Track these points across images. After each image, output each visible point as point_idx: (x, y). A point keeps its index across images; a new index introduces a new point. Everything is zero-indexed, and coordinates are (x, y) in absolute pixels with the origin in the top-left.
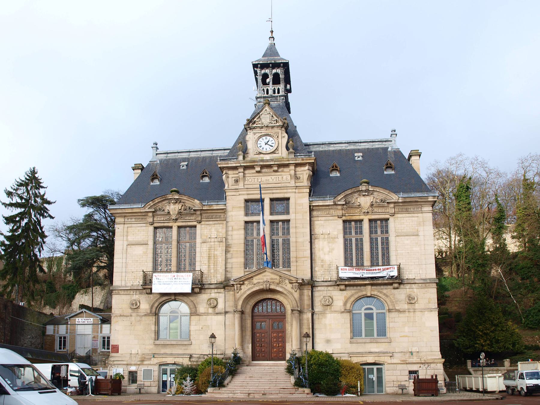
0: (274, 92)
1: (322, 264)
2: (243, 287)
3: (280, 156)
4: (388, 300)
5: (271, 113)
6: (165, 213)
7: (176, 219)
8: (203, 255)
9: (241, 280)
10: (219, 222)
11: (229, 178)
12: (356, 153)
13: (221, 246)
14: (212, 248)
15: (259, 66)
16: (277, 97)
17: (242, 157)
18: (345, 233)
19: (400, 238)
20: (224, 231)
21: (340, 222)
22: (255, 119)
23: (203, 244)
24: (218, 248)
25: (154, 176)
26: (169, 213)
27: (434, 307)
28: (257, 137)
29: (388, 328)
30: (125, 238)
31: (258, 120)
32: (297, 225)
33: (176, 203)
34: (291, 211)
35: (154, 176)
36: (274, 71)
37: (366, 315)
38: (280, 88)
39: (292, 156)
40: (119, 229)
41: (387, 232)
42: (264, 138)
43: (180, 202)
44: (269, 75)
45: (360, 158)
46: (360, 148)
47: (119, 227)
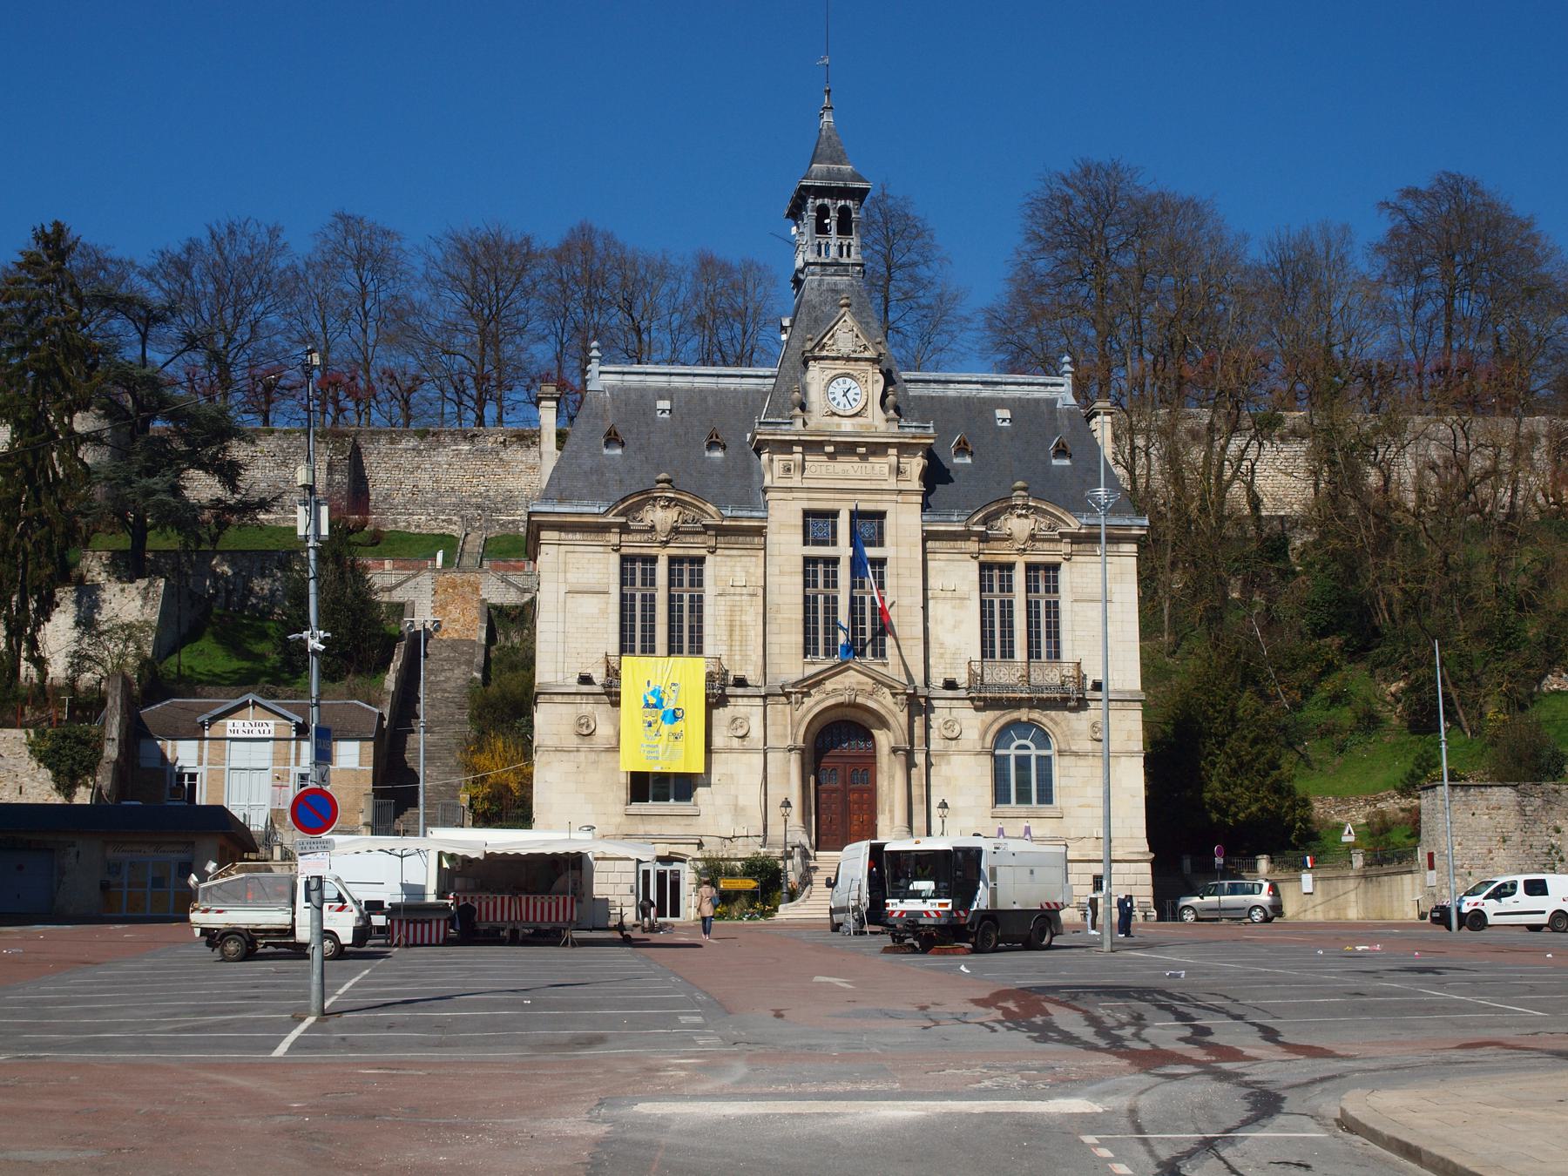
0: (841, 255)
1: (942, 651)
2: (805, 699)
3: (871, 426)
8: (719, 622)
10: (751, 552)
11: (773, 469)
12: (998, 408)
13: (754, 603)
14: (737, 608)
16: (848, 265)
21: (975, 565)
22: (825, 340)
24: (748, 608)
25: (610, 434)
26: (653, 528)
27: (1136, 749)
28: (828, 378)
29: (1058, 789)
30: (561, 575)
31: (830, 342)
33: (668, 507)
34: (888, 539)
35: (610, 434)
36: (841, 203)
39: (894, 428)
41: (1056, 590)
42: (840, 380)
43: (676, 505)
44: (831, 211)
46: (1004, 396)
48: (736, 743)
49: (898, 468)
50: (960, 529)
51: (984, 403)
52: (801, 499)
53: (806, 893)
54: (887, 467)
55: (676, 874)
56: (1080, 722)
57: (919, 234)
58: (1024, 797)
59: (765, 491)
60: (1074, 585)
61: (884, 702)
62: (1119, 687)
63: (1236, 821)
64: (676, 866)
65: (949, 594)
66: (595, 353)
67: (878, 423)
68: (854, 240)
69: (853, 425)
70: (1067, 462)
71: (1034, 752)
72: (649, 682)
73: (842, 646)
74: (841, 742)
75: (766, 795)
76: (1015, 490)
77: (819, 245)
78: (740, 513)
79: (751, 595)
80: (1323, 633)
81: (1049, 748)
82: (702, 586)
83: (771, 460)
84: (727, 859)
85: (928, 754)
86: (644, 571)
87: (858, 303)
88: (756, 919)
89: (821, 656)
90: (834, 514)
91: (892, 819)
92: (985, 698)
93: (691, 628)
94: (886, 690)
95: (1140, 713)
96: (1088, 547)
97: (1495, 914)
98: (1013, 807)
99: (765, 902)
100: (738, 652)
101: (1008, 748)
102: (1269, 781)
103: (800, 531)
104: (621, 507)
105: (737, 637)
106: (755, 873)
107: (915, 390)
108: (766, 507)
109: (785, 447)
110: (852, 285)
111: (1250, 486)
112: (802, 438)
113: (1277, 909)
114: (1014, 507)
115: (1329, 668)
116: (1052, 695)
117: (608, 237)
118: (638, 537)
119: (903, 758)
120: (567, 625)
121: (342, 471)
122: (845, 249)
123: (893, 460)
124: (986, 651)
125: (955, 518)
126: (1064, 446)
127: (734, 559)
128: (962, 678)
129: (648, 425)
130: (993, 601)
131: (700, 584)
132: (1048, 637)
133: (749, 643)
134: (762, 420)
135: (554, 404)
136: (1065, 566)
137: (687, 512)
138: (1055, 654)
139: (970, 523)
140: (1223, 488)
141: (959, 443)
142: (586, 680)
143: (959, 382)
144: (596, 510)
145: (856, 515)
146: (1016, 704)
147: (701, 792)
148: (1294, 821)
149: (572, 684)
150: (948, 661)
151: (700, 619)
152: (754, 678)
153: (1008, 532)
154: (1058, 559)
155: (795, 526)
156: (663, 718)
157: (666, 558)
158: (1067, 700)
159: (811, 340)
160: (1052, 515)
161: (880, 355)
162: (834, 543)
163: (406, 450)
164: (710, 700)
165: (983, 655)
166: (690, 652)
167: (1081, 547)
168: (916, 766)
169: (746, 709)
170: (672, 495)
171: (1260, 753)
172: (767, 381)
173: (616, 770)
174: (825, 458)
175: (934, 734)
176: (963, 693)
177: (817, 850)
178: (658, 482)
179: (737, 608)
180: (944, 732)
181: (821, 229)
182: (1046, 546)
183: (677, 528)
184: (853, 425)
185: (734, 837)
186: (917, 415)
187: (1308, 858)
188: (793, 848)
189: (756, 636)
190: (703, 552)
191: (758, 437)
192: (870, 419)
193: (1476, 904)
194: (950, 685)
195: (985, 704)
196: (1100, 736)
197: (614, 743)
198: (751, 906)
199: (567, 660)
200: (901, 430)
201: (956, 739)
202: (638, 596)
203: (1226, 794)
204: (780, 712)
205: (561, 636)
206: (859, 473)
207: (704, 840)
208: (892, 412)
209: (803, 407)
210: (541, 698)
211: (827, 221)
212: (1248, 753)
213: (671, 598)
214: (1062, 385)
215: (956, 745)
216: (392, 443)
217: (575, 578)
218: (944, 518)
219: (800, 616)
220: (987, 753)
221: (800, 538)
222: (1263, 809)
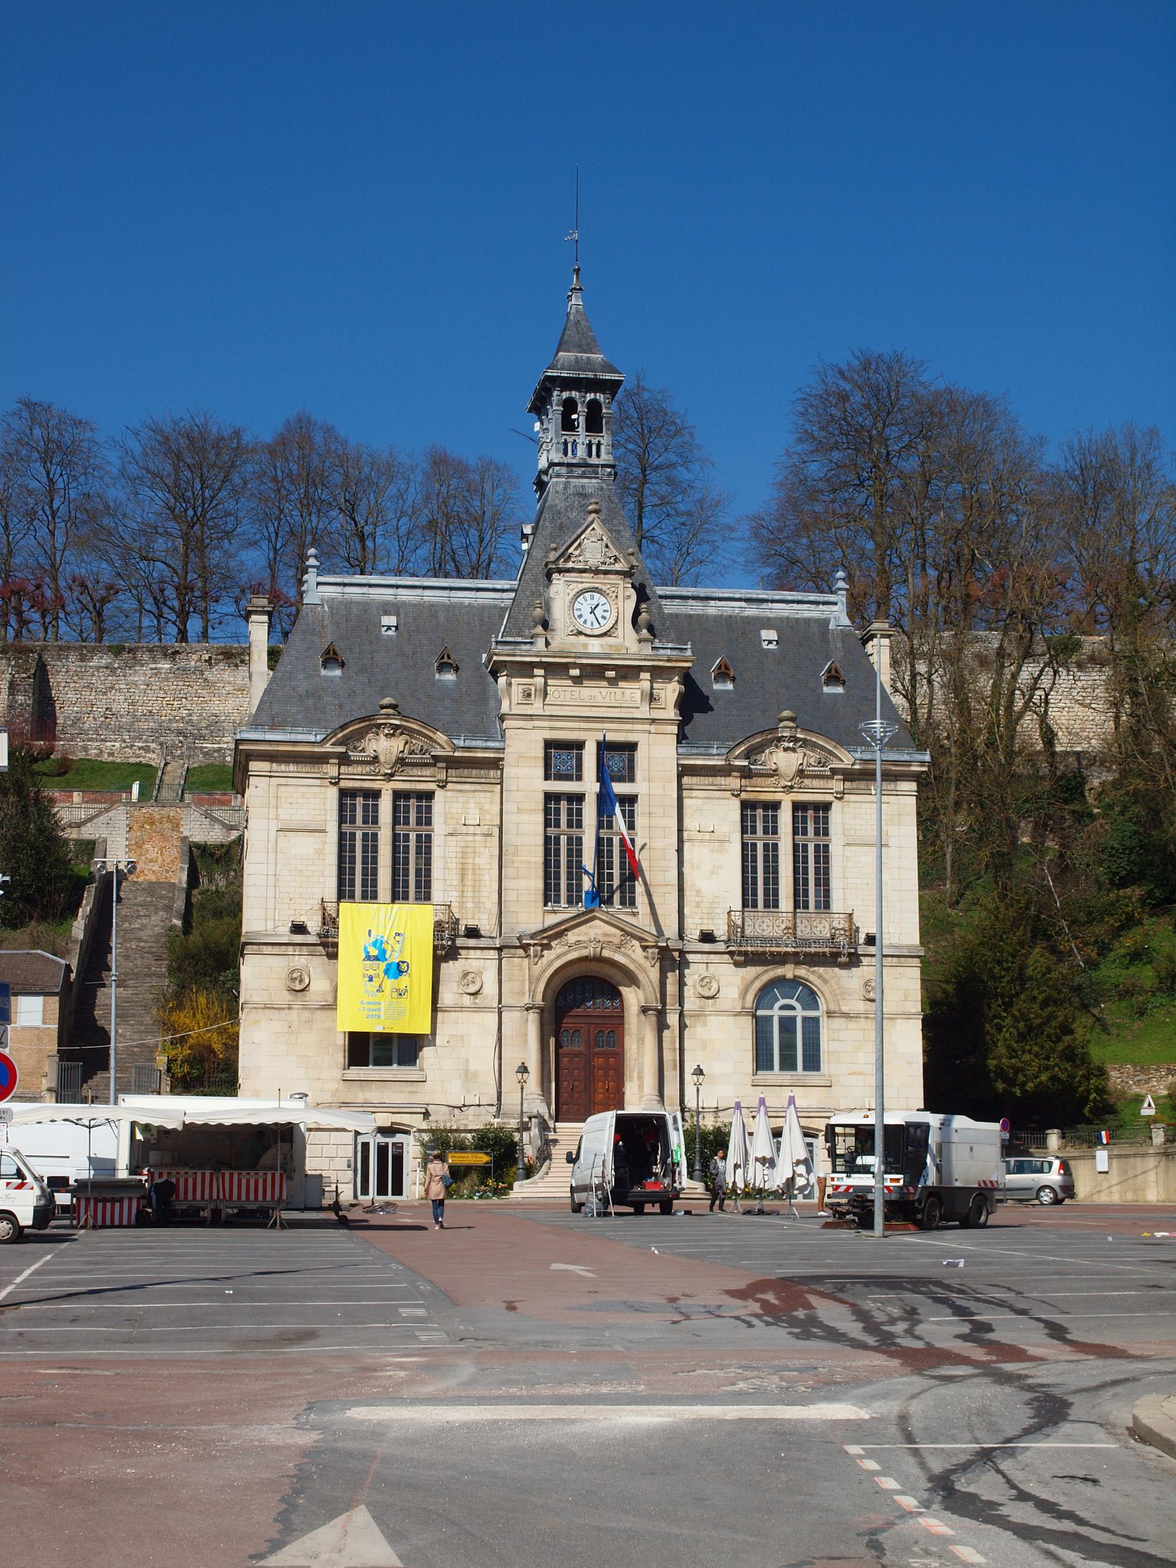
0: (590, 455)
1: (698, 899)
2: (545, 952)
3: (622, 647)
4: (825, 989)
6: (367, 756)
8: (449, 866)
9: (545, 935)
13: (489, 844)
14: (469, 850)
16: (597, 466)
19: (852, 848)
21: (736, 804)
22: (570, 551)
23: (449, 838)
24: (482, 850)
25: (328, 653)
26: (375, 760)
27: (914, 1011)
28: (574, 593)
30: (272, 811)
31: (577, 553)
32: (653, 810)
33: (393, 735)
34: (639, 774)
36: (590, 396)
37: (782, 1020)
39: (647, 649)
41: (826, 833)
42: (588, 595)
43: (402, 734)
44: (579, 406)
45: (772, 646)
46: (771, 615)
48: (467, 1001)
49: (651, 694)
52: (543, 728)
53: (544, 1169)
54: (639, 693)
55: (399, 1147)
56: (851, 980)
57: (678, 432)
58: (788, 1063)
59: (502, 718)
60: (847, 827)
61: (634, 957)
62: (895, 941)
63: (1024, 1092)
64: (399, 1138)
65: (707, 836)
66: (312, 561)
68: (605, 439)
69: (602, 645)
70: (840, 690)
71: (799, 1013)
72: (370, 931)
73: (587, 893)
74: (584, 1000)
75: (500, 1058)
76: (781, 720)
77: (566, 443)
78: (474, 743)
79: (485, 835)
80: (1123, 883)
81: (817, 1008)
83: (510, 684)
84: (457, 1131)
85: (681, 1015)
86: (365, 807)
87: (609, 510)
88: (488, 1198)
89: (563, 904)
90: (580, 745)
91: (641, 1086)
93: (418, 872)
94: (636, 943)
95: (918, 971)
96: (862, 784)
98: (776, 1075)
99: (499, 1178)
101: (771, 1008)
102: (1060, 1047)
103: (541, 764)
104: (340, 735)
106: (487, 1147)
107: (670, 607)
108: (503, 736)
109: (525, 669)
110: (601, 489)
111: (1043, 719)
112: (544, 659)
113: (1068, 1189)
114: (780, 739)
115: (1129, 922)
116: (821, 950)
117: (328, 431)
118: (359, 769)
119: (654, 1019)
120: (279, 867)
121: (26, 691)
122: (594, 448)
123: (646, 685)
124: (748, 900)
125: (714, 751)
126: (836, 671)
127: (466, 795)
128: (721, 931)
129: (371, 642)
130: (756, 844)
131: (429, 822)
132: (817, 884)
133: (483, 889)
134: (499, 639)
135: (265, 618)
136: (836, 806)
137: (414, 741)
139: (731, 757)
140: (1013, 720)
141: (719, 667)
142: (299, 929)
143: (720, 599)
144: (312, 739)
145: (604, 747)
146: (780, 959)
148: (1088, 1092)
150: (705, 910)
151: (428, 862)
152: (487, 927)
153: (774, 767)
154: (829, 798)
155: (535, 758)
156: (387, 972)
157: (390, 792)
158: (838, 955)
159: (555, 549)
160: (822, 748)
161: (632, 567)
162: (579, 778)
163: (98, 668)
164: (439, 952)
165: (745, 904)
166: (416, 899)
167: (855, 784)
168: (668, 1027)
170: (397, 722)
171: (1051, 1016)
172: (505, 595)
173: (332, 1030)
174: (569, 682)
175: (688, 992)
176: (721, 947)
177: (557, 1121)
178: (383, 707)
179: (469, 850)
180: (700, 990)
181: (568, 425)
182: (816, 783)
183: (403, 759)
184: (602, 645)
185: (464, 1106)
186: (673, 635)
188: (530, 1118)
189: (491, 881)
190: (432, 786)
191: (495, 658)
192: (621, 640)
194: (707, 937)
196: (874, 995)
197: (330, 1000)
198: (483, 1183)
200: (655, 652)
201: (713, 997)
203: (1013, 1061)
204: (516, 965)
206: (606, 700)
207: (431, 1109)
208: (645, 631)
209: (545, 625)
210: (249, 949)
211: (574, 416)
212: (1038, 1016)
213: (395, 838)
214: (835, 604)
215: (713, 1004)
216: (82, 660)
217: (285, 814)
218: (702, 750)
219: (540, 859)
220: (748, 1013)
221: (540, 771)
222: (1053, 1078)
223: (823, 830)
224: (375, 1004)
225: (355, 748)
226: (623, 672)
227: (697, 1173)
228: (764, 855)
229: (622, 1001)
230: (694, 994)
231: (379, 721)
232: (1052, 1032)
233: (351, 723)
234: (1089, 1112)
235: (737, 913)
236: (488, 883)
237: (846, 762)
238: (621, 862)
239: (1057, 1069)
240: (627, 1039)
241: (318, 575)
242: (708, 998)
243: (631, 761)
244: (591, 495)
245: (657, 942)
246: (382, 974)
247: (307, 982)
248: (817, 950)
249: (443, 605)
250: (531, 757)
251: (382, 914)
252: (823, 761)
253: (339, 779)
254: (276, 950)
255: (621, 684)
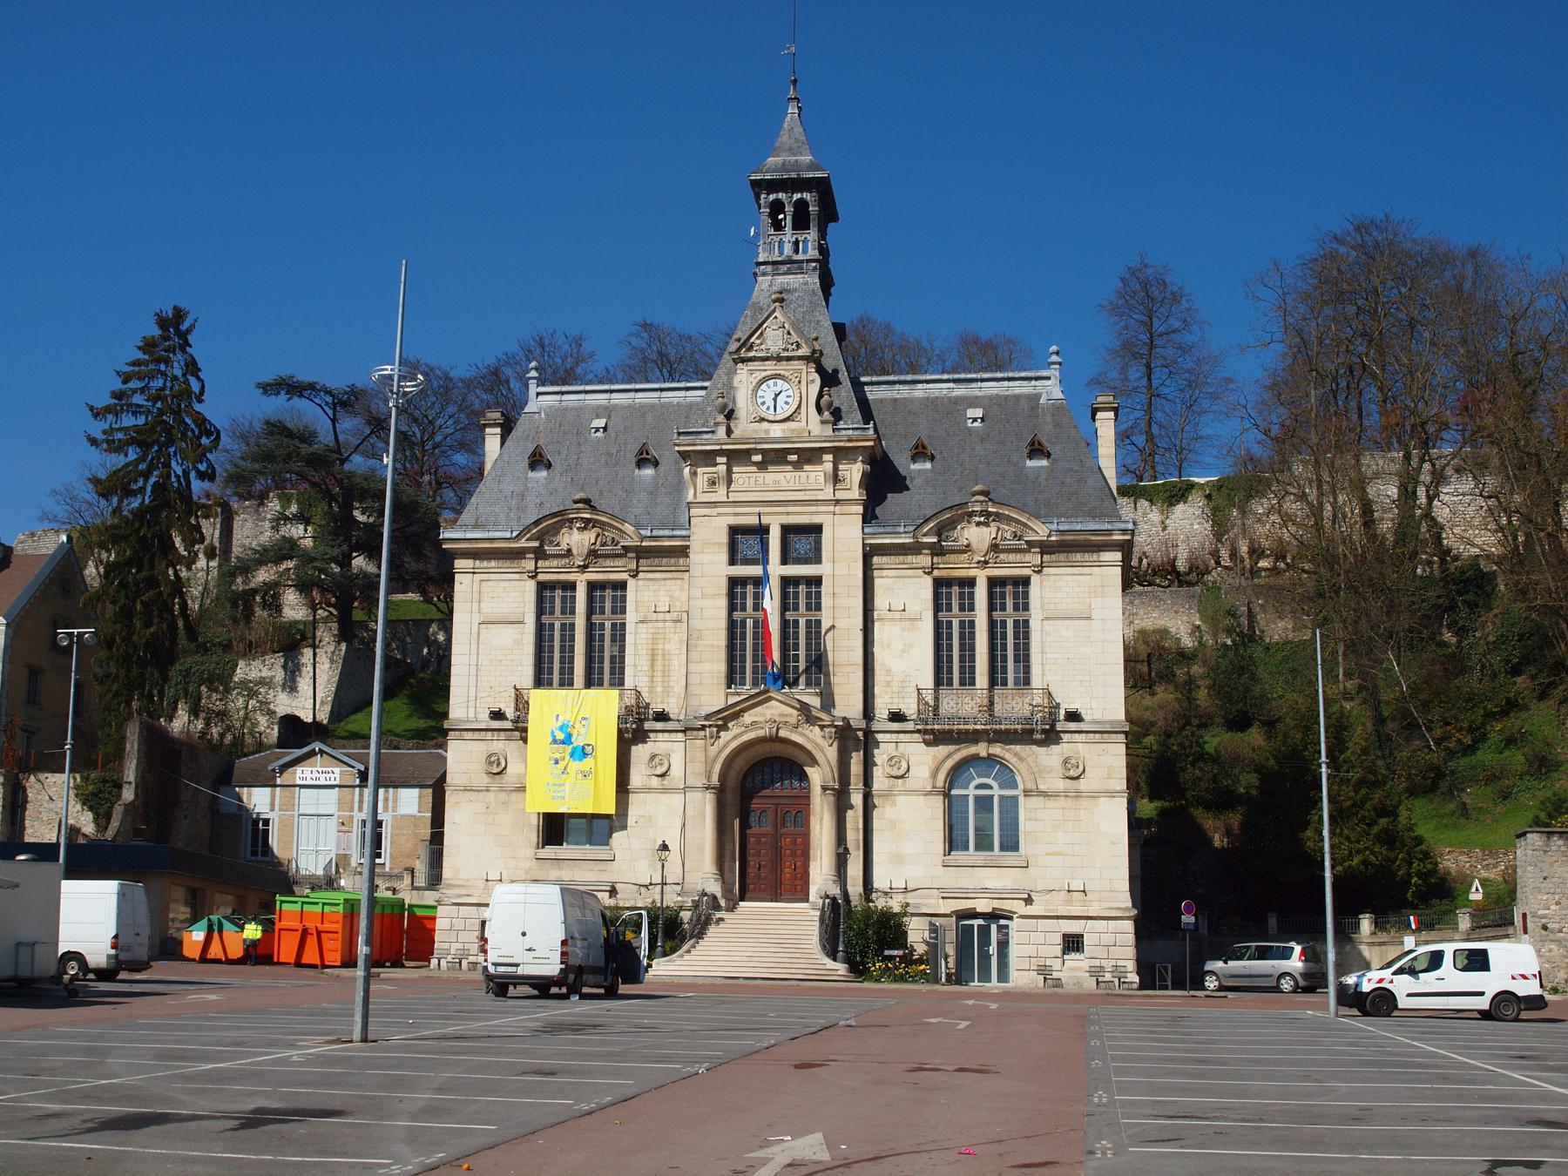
0: (797, 251)
1: (888, 678)
2: (722, 734)
4: (1022, 767)
5: (786, 325)
7: (585, 566)
12: (970, 407)
14: (659, 636)
15: (764, 184)
16: (802, 261)
17: (724, 428)
18: (937, 608)
20: (685, 595)
22: (751, 341)
23: (640, 625)
24: (672, 635)
25: (535, 456)
26: (569, 550)
27: (1118, 789)
28: (756, 381)
30: (475, 605)
31: (758, 342)
33: (585, 528)
34: (824, 555)
35: (535, 456)
36: (797, 196)
38: (809, 238)
39: (828, 430)
40: (464, 586)
41: (1026, 608)
43: (593, 527)
46: (980, 394)
47: (464, 581)
48: (655, 782)
50: (907, 541)
51: (955, 403)
52: (727, 514)
54: (822, 474)
56: (1050, 757)
58: (984, 843)
62: (1098, 716)
65: (898, 615)
66: (534, 374)
67: (813, 427)
69: (784, 431)
71: (996, 792)
74: (772, 783)
78: (661, 533)
81: (1016, 787)
82: (625, 613)
83: (695, 474)
85: (867, 797)
86: (564, 598)
87: (811, 302)
92: (933, 730)
93: (613, 658)
95: (1123, 747)
96: (1062, 556)
97: (1409, 995)
98: (971, 855)
100: (659, 684)
101: (967, 788)
102: (1375, 830)
105: (659, 666)
109: (708, 458)
112: (724, 447)
114: (971, 514)
116: (1012, 727)
118: (555, 562)
119: (831, 798)
123: (829, 466)
124: (941, 676)
126: (1040, 444)
127: (657, 583)
128: (910, 708)
130: (951, 622)
131: (623, 611)
132: (1016, 661)
135: (498, 430)
136: (1035, 579)
138: (1025, 680)
142: (497, 715)
143: (928, 382)
144: (508, 535)
145: (787, 530)
147: (618, 837)
148: (1410, 876)
149: (484, 719)
151: (622, 650)
153: (965, 542)
154: (1027, 572)
155: (719, 544)
156: (572, 755)
157: (584, 583)
158: (1031, 731)
160: (1018, 522)
165: (938, 682)
166: (611, 685)
167: (1054, 557)
168: (852, 807)
169: (664, 745)
170: (588, 516)
174: (754, 469)
175: (877, 772)
176: (910, 726)
180: (888, 770)
181: (778, 226)
182: (1012, 557)
184: (784, 431)
185: (651, 884)
187: (1412, 918)
189: (680, 665)
190: (624, 576)
193: (1381, 981)
194: (897, 717)
195: (936, 738)
199: (479, 695)
201: (902, 777)
202: (557, 625)
205: (473, 669)
207: (618, 887)
208: (826, 413)
211: (781, 216)
214: (1049, 378)
215: (903, 784)
217: (490, 608)
220: (938, 793)
221: (724, 556)
222: (1365, 862)
223: (1023, 605)
224: (560, 785)
225: (552, 542)
226: (808, 455)
227: (840, 954)
228: (960, 633)
229: (809, 782)
230: (883, 773)
231: (571, 516)
232: (1367, 814)
233: (544, 518)
234: (1413, 896)
235: (930, 691)
236: (677, 668)
237: (1041, 534)
238: (807, 644)
239: (1368, 852)
240: (812, 819)
241: (538, 386)
242: (897, 777)
243: (818, 544)
244: (795, 290)
245: (833, 721)
246: (568, 758)
247: (503, 765)
248: (1008, 727)
249: (653, 406)
250: (715, 544)
251: (570, 698)
252: (1019, 534)
253: (537, 573)
254: (477, 735)
255: (807, 467)
